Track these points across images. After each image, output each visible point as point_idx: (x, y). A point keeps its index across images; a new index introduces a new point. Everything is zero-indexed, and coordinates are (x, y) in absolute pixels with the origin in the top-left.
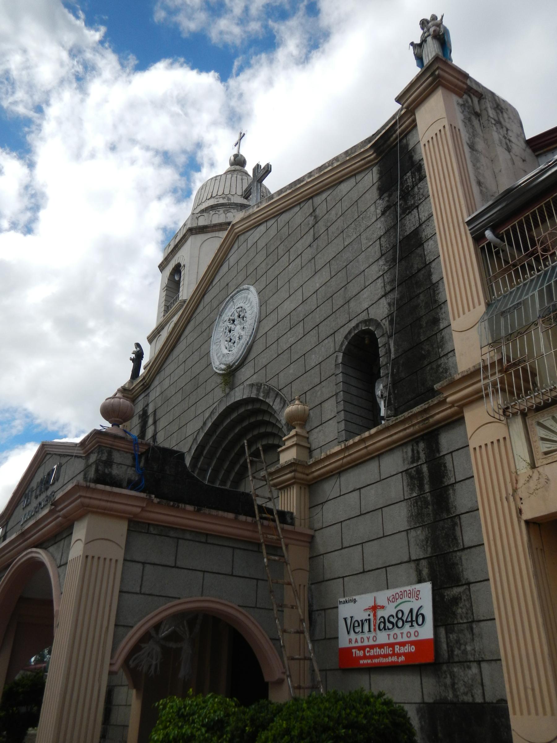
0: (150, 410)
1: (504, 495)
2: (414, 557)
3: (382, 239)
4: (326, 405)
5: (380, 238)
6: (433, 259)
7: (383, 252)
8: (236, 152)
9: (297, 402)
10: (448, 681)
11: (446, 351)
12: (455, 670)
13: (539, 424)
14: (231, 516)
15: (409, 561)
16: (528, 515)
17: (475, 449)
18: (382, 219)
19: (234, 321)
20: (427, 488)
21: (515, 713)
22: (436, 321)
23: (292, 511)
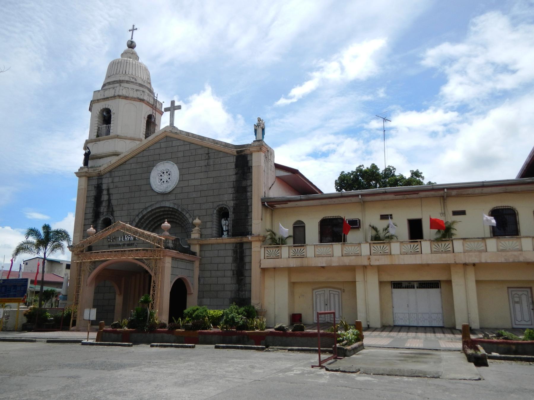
0: (104, 187)
1: (258, 262)
2: (232, 269)
3: (234, 182)
4: (208, 223)
5: (234, 181)
6: (249, 198)
7: (234, 186)
8: (130, 39)
9: (197, 219)
10: (238, 294)
11: (248, 224)
12: (240, 292)
13: (267, 250)
14: (188, 255)
15: (231, 270)
16: (261, 267)
17: (253, 251)
18: (235, 176)
19: (163, 173)
20: (238, 255)
21: (252, 299)
22: (247, 216)
23: (196, 251)
